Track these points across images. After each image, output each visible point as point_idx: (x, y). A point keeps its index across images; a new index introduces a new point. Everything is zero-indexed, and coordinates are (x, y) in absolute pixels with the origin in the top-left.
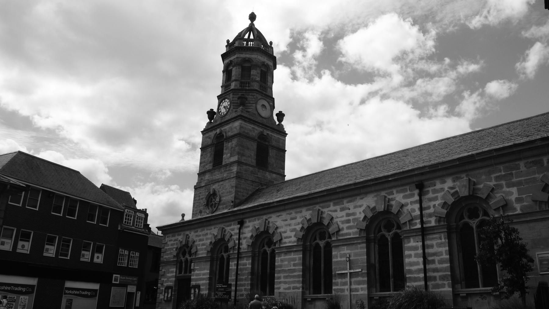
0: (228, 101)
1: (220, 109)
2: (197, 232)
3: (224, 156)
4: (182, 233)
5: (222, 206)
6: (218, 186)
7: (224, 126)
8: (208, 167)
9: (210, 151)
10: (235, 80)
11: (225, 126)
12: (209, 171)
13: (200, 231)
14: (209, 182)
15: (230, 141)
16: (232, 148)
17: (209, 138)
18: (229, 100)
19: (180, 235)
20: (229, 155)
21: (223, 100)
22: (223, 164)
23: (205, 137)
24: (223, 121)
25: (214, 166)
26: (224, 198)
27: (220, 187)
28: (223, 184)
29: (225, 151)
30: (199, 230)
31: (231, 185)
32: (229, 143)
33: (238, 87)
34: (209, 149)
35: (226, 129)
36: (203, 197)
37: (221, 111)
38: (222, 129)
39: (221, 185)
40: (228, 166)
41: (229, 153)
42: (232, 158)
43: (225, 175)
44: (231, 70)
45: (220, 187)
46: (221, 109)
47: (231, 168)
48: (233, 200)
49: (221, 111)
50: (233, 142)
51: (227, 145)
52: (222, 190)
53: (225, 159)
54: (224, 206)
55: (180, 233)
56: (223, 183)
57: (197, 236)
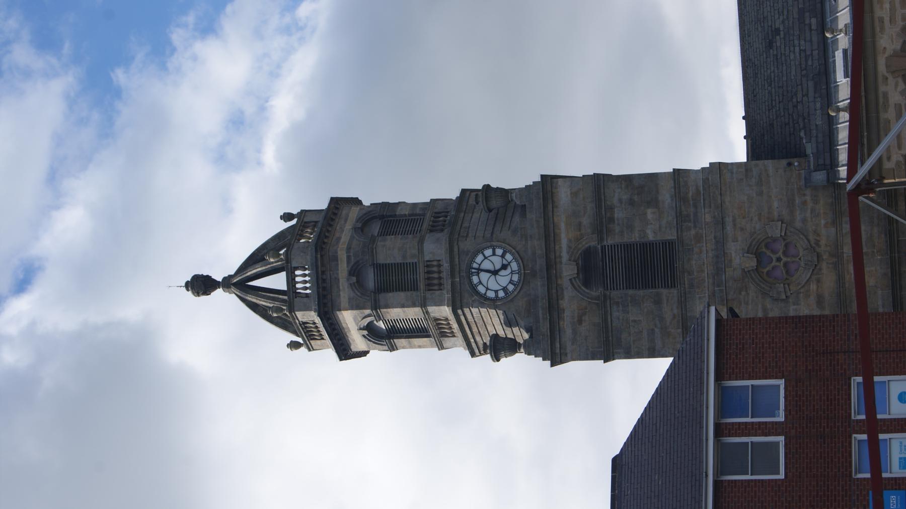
0: (479, 258)
1: (496, 292)
2: (881, 20)
3: (651, 237)
4: (882, 88)
5: (798, 212)
6: (735, 240)
7: (557, 254)
8: (672, 309)
9: (621, 308)
10: (421, 242)
11: (557, 247)
12: (683, 302)
13: (882, 8)
14: (718, 286)
15: (608, 215)
16: (631, 203)
17: (580, 322)
18: (475, 255)
19: (885, 95)
20: (650, 214)
21: (471, 281)
22: (671, 235)
23: (573, 344)
24: (541, 263)
25: (671, 281)
26: (776, 204)
27: (742, 229)
28: (734, 221)
29: (635, 237)
30: (878, 13)
31: (742, 179)
32: (612, 220)
33: (443, 236)
34: (615, 314)
35: (570, 241)
36: (760, 306)
37: (505, 289)
38: (565, 256)
39: (735, 225)
40: (683, 208)
41: (645, 214)
42: (660, 198)
43: (708, 218)
44: (381, 268)
45: (742, 229)
46: (498, 288)
47: (690, 194)
48: (784, 162)
49: (505, 289)
50: (615, 201)
51: (617, 229)
52: (752, 220)
53: (660, 227)
54: (797, 201)
55: (881, 100)
56: (731, 219)
57: (892, 20)
